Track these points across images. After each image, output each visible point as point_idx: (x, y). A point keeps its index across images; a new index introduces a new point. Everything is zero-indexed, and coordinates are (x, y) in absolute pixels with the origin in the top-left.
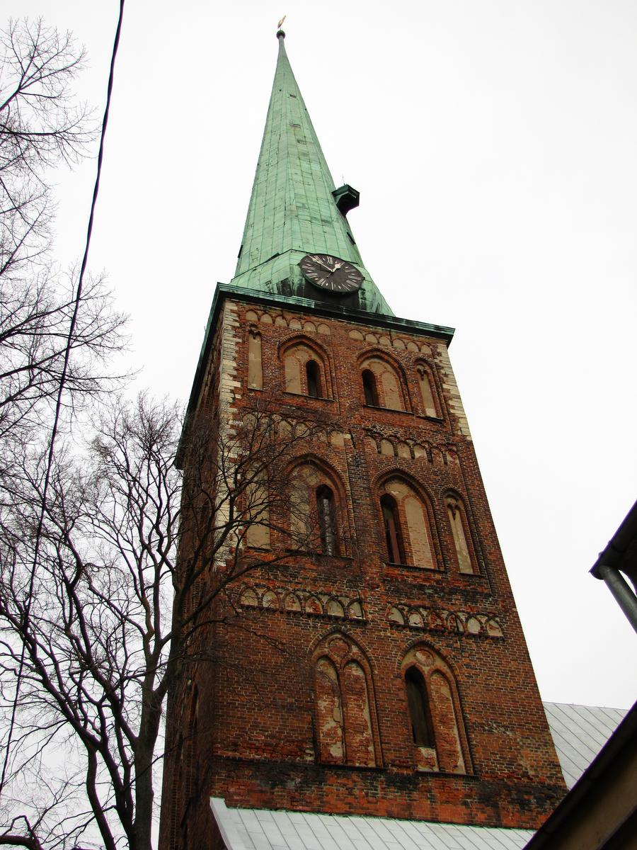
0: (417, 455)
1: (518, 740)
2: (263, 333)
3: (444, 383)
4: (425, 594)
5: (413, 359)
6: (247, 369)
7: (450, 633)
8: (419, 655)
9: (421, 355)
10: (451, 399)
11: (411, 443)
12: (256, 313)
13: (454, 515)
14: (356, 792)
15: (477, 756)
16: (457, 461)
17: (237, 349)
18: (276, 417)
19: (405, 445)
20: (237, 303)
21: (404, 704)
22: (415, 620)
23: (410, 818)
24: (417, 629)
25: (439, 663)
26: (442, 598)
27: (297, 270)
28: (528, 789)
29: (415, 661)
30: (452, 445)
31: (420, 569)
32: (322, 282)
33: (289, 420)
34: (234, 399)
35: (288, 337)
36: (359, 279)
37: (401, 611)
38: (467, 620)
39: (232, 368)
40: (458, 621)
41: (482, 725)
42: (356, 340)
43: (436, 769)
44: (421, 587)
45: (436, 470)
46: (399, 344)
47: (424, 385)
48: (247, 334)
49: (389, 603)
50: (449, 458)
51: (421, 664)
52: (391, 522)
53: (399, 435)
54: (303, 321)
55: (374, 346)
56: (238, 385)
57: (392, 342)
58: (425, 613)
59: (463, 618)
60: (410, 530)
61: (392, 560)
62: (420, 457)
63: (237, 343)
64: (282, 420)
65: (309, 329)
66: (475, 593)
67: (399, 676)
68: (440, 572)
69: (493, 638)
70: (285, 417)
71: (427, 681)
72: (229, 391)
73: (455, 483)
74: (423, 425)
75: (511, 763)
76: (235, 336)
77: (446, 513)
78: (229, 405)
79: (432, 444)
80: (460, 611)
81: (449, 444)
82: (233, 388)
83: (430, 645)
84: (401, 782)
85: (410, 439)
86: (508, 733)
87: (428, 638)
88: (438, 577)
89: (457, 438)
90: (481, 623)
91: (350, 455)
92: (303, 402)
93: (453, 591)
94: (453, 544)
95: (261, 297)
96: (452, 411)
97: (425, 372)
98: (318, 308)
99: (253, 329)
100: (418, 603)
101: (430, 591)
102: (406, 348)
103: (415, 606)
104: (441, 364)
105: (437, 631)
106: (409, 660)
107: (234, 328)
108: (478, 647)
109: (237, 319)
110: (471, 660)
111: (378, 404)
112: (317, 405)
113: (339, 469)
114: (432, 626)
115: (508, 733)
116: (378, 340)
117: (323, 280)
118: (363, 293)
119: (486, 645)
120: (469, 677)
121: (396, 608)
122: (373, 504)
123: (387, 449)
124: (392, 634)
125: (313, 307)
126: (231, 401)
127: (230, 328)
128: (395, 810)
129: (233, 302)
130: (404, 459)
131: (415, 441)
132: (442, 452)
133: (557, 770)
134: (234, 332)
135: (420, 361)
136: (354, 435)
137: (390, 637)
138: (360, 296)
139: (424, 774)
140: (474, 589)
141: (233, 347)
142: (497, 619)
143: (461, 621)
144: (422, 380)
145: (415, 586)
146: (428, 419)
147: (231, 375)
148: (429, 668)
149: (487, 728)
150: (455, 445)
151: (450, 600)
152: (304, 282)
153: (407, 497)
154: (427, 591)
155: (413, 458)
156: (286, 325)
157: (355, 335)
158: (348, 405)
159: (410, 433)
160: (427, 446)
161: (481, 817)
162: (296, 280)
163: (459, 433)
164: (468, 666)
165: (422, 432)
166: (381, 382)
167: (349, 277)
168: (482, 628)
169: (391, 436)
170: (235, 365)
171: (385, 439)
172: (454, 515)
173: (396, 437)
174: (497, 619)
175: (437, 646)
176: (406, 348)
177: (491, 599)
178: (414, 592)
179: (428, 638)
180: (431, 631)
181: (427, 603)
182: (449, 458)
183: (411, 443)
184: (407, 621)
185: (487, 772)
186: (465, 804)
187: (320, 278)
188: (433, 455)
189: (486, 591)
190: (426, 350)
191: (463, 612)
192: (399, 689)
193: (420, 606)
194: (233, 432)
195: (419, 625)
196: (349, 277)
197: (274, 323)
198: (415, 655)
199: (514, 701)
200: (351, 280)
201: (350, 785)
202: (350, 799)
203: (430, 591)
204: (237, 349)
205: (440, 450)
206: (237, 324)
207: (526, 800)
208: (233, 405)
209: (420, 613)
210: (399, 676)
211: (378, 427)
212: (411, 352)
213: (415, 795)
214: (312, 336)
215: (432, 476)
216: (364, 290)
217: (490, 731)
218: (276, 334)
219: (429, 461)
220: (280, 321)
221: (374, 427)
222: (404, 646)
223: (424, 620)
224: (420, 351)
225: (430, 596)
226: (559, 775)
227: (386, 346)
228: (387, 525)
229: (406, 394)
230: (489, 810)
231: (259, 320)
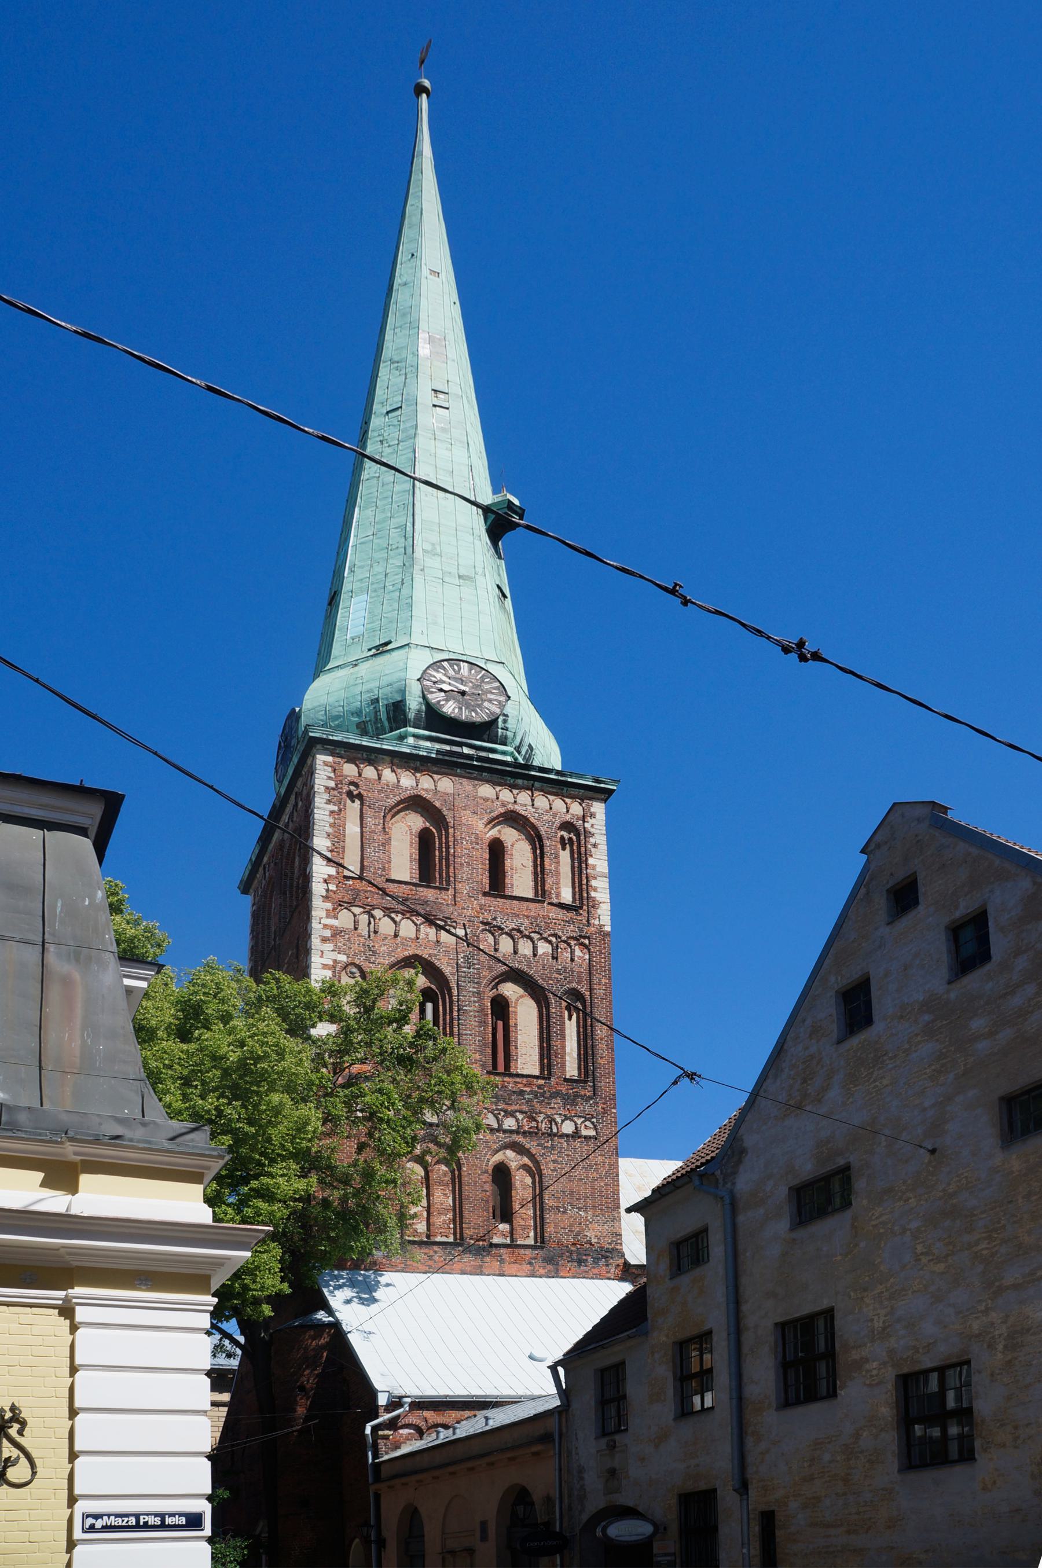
0: (540, 951)
1: (589, 1218)
2: (364, 793)
3: (591, 856)
4: (525, 1099)
5: (557, 823)
6: (343, 847)
7: (543, 1134)
8: (510, 1153)
9: (568, 818)
10: (595, 878)
11: (535, 936)
13: (570, 1018)
14: (436, 1258)
15: (548, 1230)
16: (587, 957)
17: (332, 821)
18: (378, 913)
19: (529, 941)
20: (332, 754)
21: (488, 1193)
22: (509, 1123)
23: (481, 1273)
24: (511, 1132)
25: (526, 1160)
26: (541, 1102)
28: (588, 1253)
29: (504, 1158)
30: (585, 937)
31: (523, 1076)
32: (450, 708)
33: (393, 915)
34: (328, 890)
35: (398, 798)
36: (503, 699)
37: (496, 1116)
38: (563, 1121)
40: (553, 1123)
41: (558, 1208)
42: (486, 800)
43: (508, 1242)
44: (521, 1093)
45: (560, 967)
46: (542, 801)
47: (565, 856)
48: (344, 796)
49: (485, 1108)
50: (578, 952)
51: (510, 1160)
52: (500, 1023)
53: (522, 929)
54: (418, 775)
55: (510, 807)
57: (533, 800)
58: (520, 1116)
59: (559, 1120)
60: (519, 1032)
61: (495, 1065)
62: (543, 953)
63: (332, 812)
64: (384, 916)
65: (426, 786)
66: (577, 1095)
67: (486, 1172)
68: (543, 1078)
69: (585, 1137)
71: (513, 1173)
72: (322, 880)
73: (578, 983)
74: (555, 913)
75: (577, 1235)
76: (329, 802)
77: (562, 1017)
78: (321, 899)
79: (560, 938)
80: (557, 1114)
81: (581, 936)
83: (521, 1145)
84: (475, 1250)
85: (535, 932)
86: (580, 1213)
87: (520, 1139)
88: (541, 1082)
89: (593, 929)
90: (576, 1124)
91: (462, 955)
92: (411, 890)
93: (555, 1095)
94: (564, 1047)
95: (364, 743)
96: (593, 894)
97: (570, 839)
98: (440, 757)
99: (352, 788)
100: (517, 1107)
101: (530, 1096)
102: (551, 808)
103: (512, 1111)
104: (592, 830)
105: (530, 1133)
106: (498, 1157)
108: (568, 1144)
109: (332, 775)
110: (558, 1157)
111: (504, 892)
112: (429, 894)
113: (447, 970)
114: (526, 1128)
115: (580, 1213)
117: (451, 703)
118: (505, 721)
119: (577, 1143)
120: (555, 1170)
121: (492, 1113)
122: (482, 1010)
123: (506, 945)
124: (484, 1136)
125: (434, 756)
126: (324, 893)
127: (322, 789)
128: (468, 1269)
129: (327, 749)
130: (524, 956)
131: (541, 934)
132: (571, 947)
133: (618, 1238)
134: (326, 796)
135: (567, 826)
136: (468, 931)
137: (482, 1139)
138: (500, 724)
139: (497, 1246)
140: (577, 1092)
141: (327, 818)
142: (594, 1120)
143: (556, 1124)
144: (564, 849)
145: (514, 1092)
146: (561, 906)
148: (516, 1163)
149: (562, 1210)
150: (588, 938)
151: (549, 1104)
153: (522, 997)
154: (527, 1097)
155: (535, 955)
156: (396, 781)
158: (465, 892)
159: (537, 925)
160: (554, 939)
161: (542, 1271)
163: (596, 922)
164: (555, 1161)
165: (551, 923)
166: (512, 855)
167: (490, 696)
168: (576, 1128)
169: (513, 929)
170: (328, 844)
171: (506, 933)
172: (570, 1018)
173: (519, 931)
174: (594, 1120)
175: (528, 1146)
176: (551, 808)
177: (591, 1102)
178: (513, 1097)
179: (520, 1139)
180: (524, 1133)
181: (525, 1108)
182: (578, 952)
183: (535, 936)
184: (500, 1125)
185: (554, 1242)
186: (530, 1263)
187: (447, 700)
188: (559, 950)
189: (588, 1094)
190: (576, 808)
191: (560, 1114)
192: (485, 1183)
193: (516, 1111)
194: (328, 933)
195: (514, 1128)
196: (490, 696)
197: (380, 779)
198: (505, 1153)
199: (593, 1188)
200: (490, 701)
201: (431, 1253)
202: (430, 1263)
203: (530, 1096)
204: (332, 821)
205: (569, 945)
206: (332, 784)
207: (584, 1260)
208: (326, 898)
209: (515, 1117)
210: (486, 1172)
211: (499, 919)
212: (555, 815)
213: (488, 1259)
215: (555, 975)
216: (507, 716)
217: (564, 1212)
218: (383, 795)
219: (553, 958)
221: (495, 919)
222: (495, 1146)
223: (518, 1123)
224: (568, 811)
225: (529, 1101)
226: (619, 1241)
227: (526, 805)
228: (494, 1035)
229: (540, 874)
230: (550, 1267)
231: (360, 775)
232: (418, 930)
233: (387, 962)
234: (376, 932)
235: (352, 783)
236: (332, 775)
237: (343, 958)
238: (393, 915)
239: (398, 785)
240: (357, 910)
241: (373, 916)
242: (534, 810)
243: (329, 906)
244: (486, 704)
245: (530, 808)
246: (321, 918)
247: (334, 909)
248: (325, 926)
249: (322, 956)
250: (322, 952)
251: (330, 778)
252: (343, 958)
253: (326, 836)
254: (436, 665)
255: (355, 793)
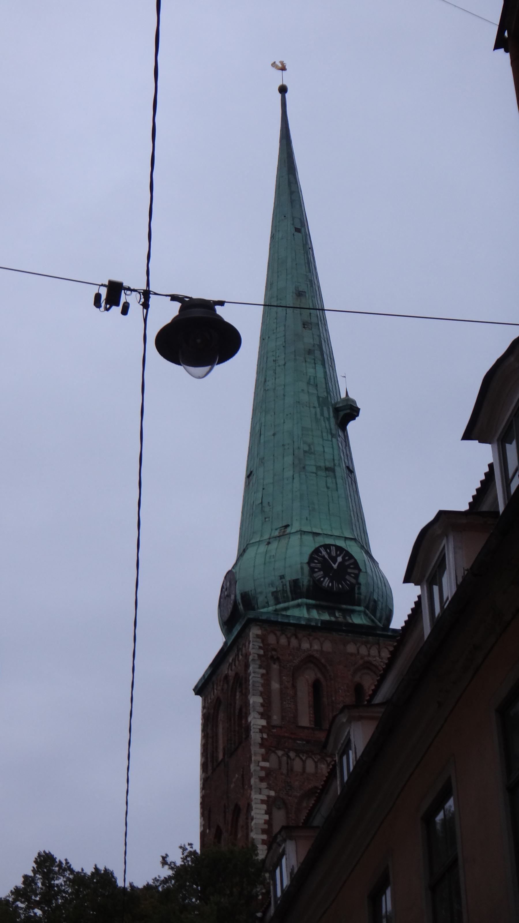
12: (275, 634)
17: (262, 681)
18: (292, 754)
27: (306, 569)
32: (326, 582)
34: (262, 738)
36: (356, 572)
39: (259, 704)
42: (352, 654)
55: (366, 658)
56: (263, 722)
57: (379, 652)
70: (298, 752)
76: (260, 667)
82: (260, 727)
107: (259, 656)
109: (261, 645)
116: (369, 651)
117: (327, 579)
126: (259, 741)
141: (259, 680)
147: (260, 713)
152: (312, 583)
157: (351, 648)
162: (305, 581)
167: (349, 571)
194: (263, 774)
196: (349, 571)
200: (349, 574)
204: (262, 681)
208: (262, 745)
214: (317, 655)
220: (294, 642)
227: (375, 657)
231: (278, 643)
232: (316, 767)
233: (298, 795)
234: (292, 770)
235: (274, 650)
236: (261, 645)
237: (272, 793)
238: (301, 756)
239: (299, 648)
240: (280, 753)
241: (288, 757)
242: (380, 660)
243: (263, 751)
244: (347, 577)
245: (378, 658)
246: (259, 762)
247: (267, 753)
248: (263, 768)
249: (260, 793)
250: (260, 789)
251: (260, 648)
252: (272, 793)
253: (259, 694)
254: (317, 551)
255: (275, 657)
